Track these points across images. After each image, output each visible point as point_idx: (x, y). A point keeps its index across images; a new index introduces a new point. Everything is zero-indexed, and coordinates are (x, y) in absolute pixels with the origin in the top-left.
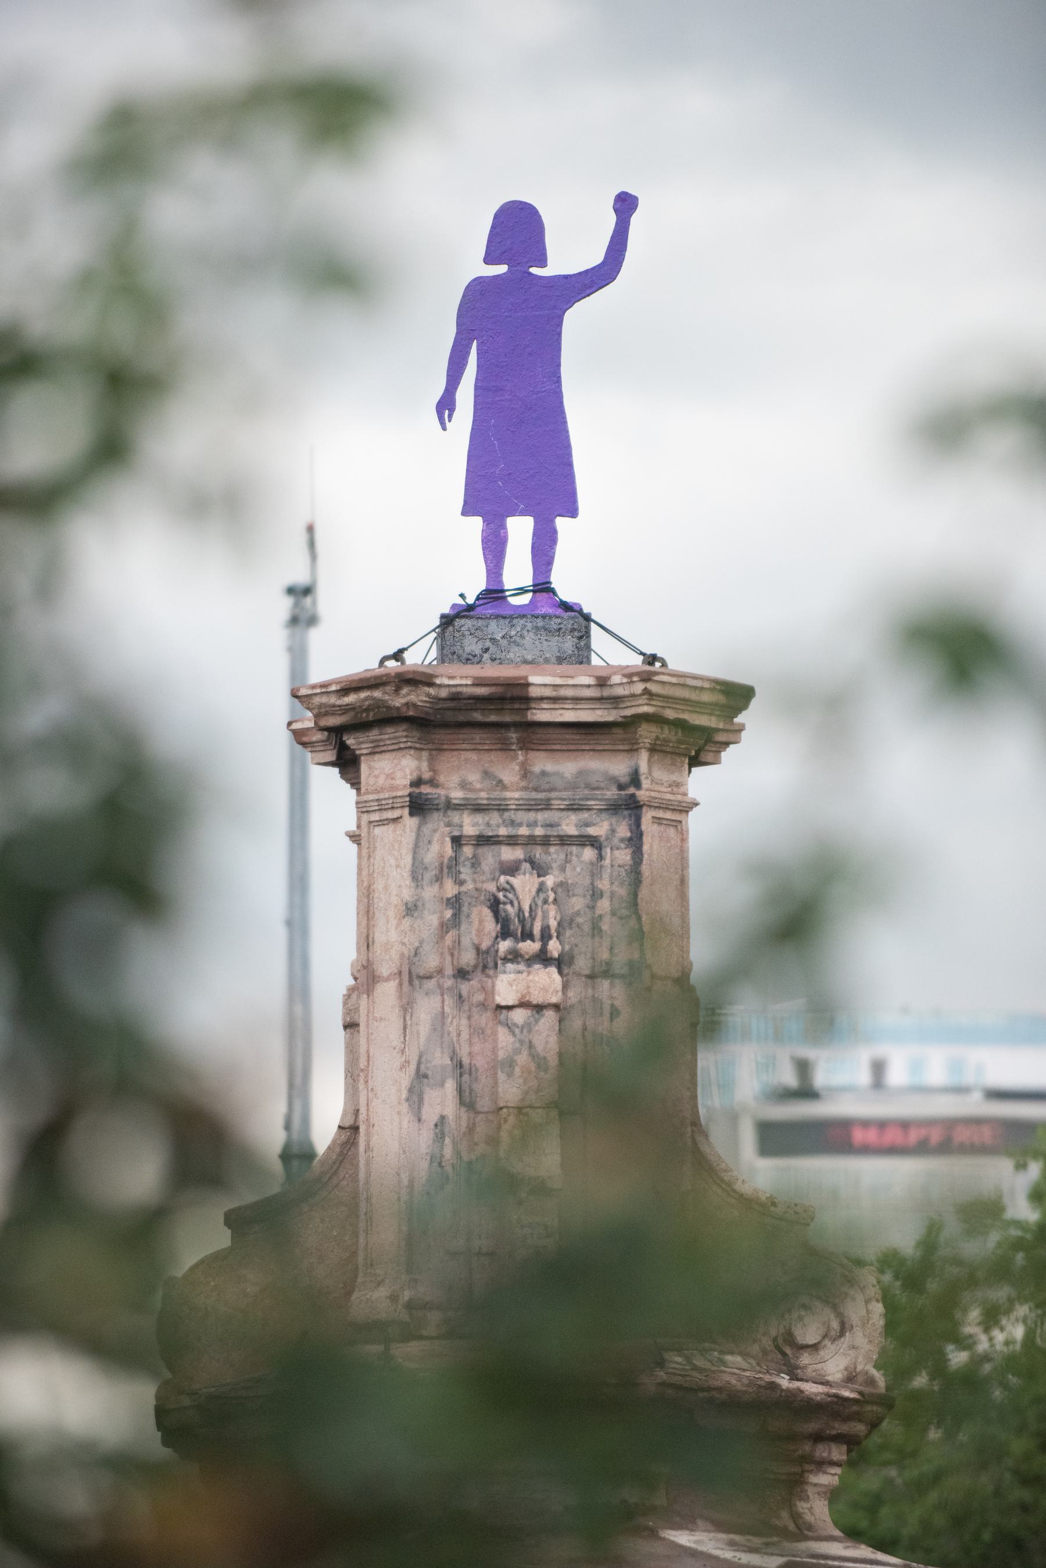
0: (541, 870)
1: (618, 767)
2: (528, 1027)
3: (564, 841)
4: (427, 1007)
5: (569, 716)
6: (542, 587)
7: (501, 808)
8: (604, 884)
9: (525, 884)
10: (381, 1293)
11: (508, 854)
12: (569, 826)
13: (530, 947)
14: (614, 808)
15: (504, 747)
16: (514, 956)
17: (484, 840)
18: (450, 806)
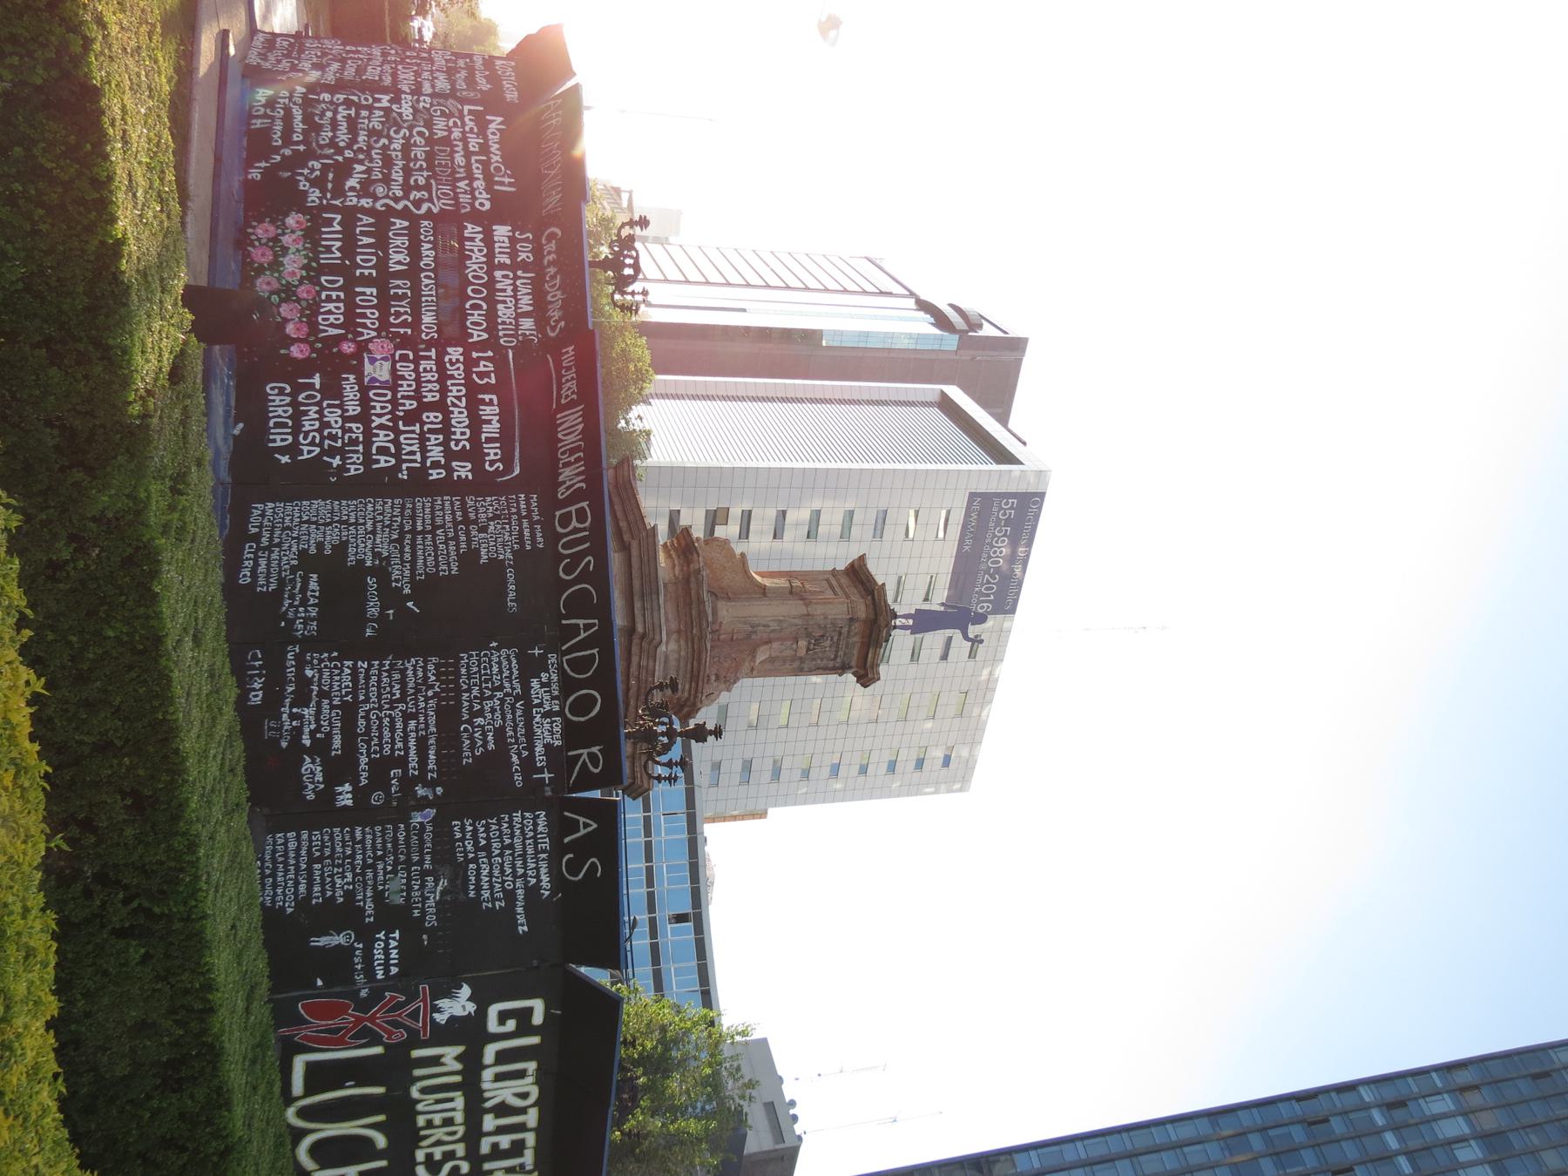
0: (830, 647)
1: (853, 663)
2: (792, 648)
3: (837, 651)
4: (798, 621)
5: (870, 655)
6: (895, 627)
7: (848, 637)
8: (825, 661)
9: (828, 643)
10: (725, 613)
11: (835, 639)
12: (841, 653)
13: (812, 647)
14: (843, 662)
15: (863, 637)
16: (810, 643)
17: (840, 633)
18: (850, 626)
